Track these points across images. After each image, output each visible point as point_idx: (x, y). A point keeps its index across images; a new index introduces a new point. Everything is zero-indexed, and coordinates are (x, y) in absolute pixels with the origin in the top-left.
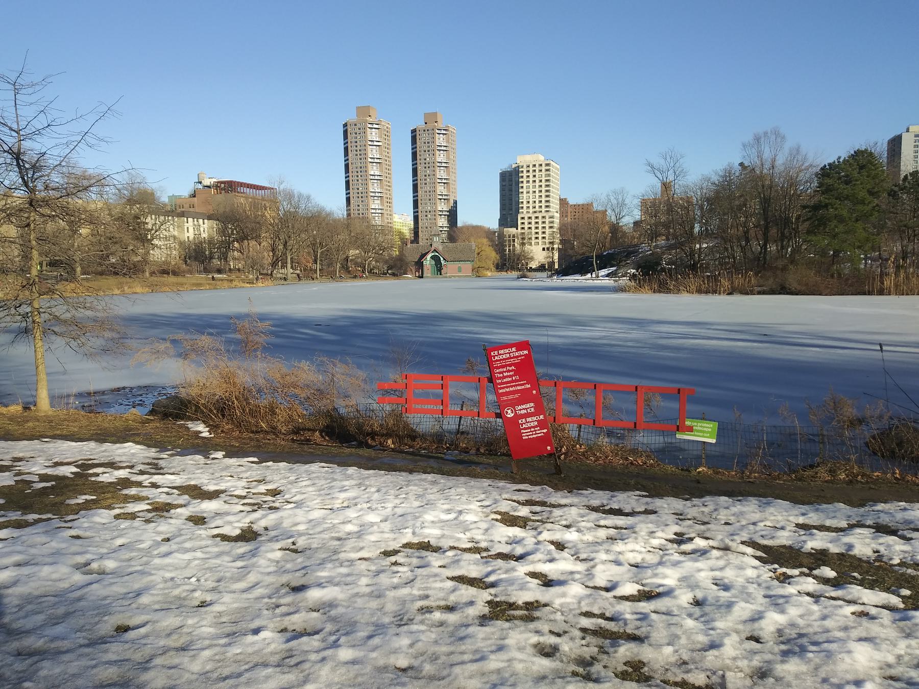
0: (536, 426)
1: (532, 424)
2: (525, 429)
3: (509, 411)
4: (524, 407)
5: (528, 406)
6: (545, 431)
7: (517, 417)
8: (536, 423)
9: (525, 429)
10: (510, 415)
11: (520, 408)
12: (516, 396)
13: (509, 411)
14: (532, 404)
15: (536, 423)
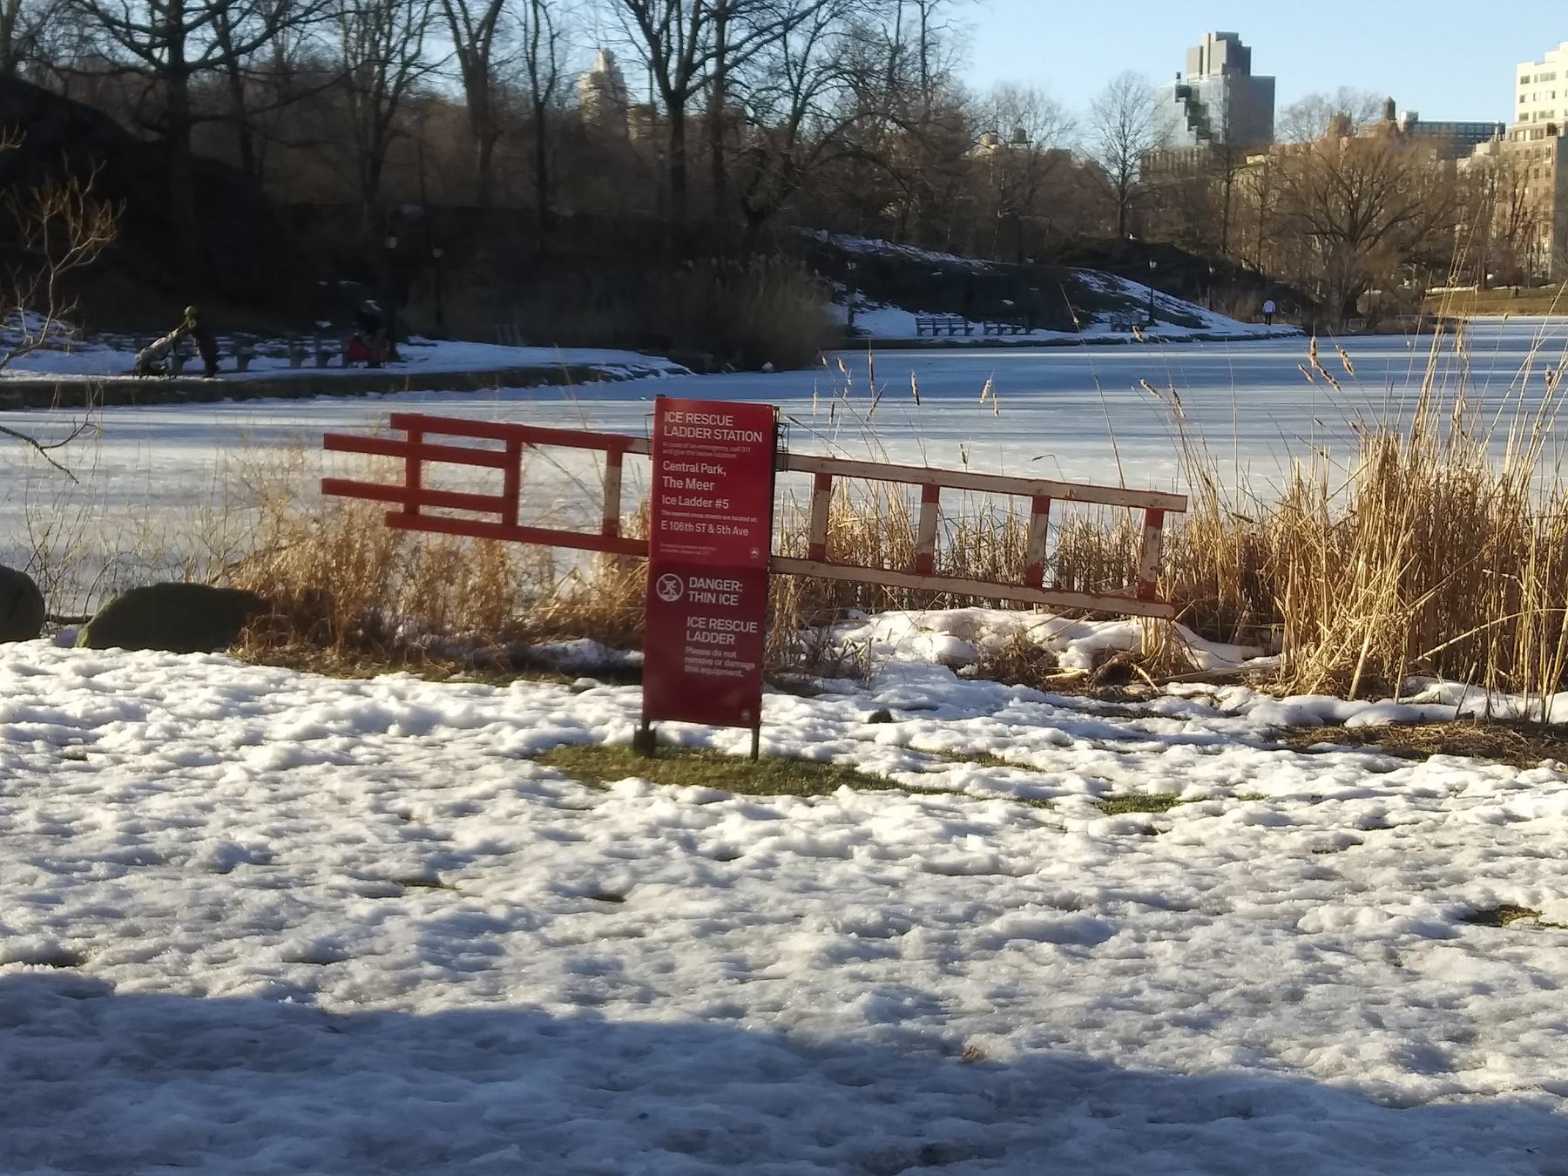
0: (728, 648)
1: (720, 638)
2: (697, 645)
3: (670, 585)
4: (713, 584)
5: (724, 586)
6: (749, 666)
7: (687, 607)
8: (731, 640)
9: (697, 645)
10: (670, 596)
11: (700, 583)
12: (705, 551)
13: (670, 585)
14: (736, 585)
15: (731, 640)
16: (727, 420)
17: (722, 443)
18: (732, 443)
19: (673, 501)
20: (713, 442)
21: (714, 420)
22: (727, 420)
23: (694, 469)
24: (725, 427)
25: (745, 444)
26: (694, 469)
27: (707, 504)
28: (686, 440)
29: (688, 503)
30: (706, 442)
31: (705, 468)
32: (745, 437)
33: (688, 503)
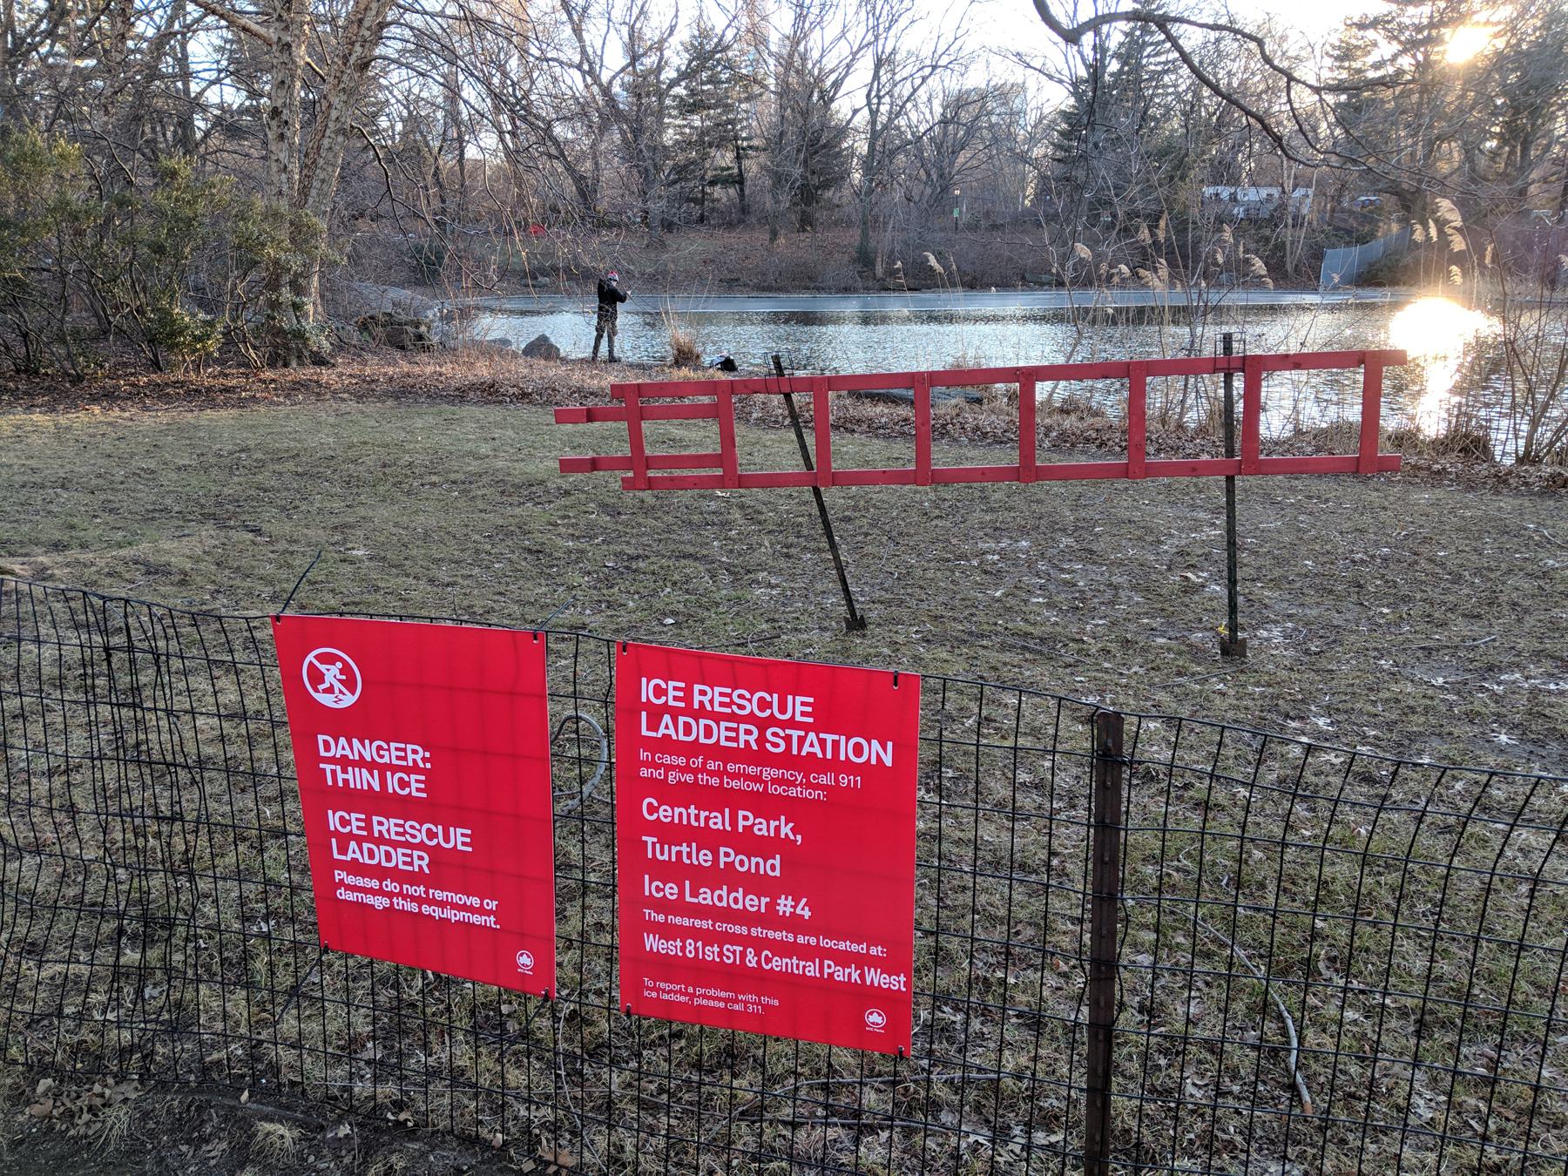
16: (799, 706)
17: (786, 760)
18: (810, 764)
19: (671, 891)
20: (761, 756)
21: (763, 705)
22: (799, 706)
23: (718, 822)
24: (792, 723)
25: (849, 767)
26: (718, 822)
27: (753, 903)
28: (693, 749)
29: (706, 897)
30: (745, 755)
31: (745, 819)
32: (846, 750)
33: (706, 897)
